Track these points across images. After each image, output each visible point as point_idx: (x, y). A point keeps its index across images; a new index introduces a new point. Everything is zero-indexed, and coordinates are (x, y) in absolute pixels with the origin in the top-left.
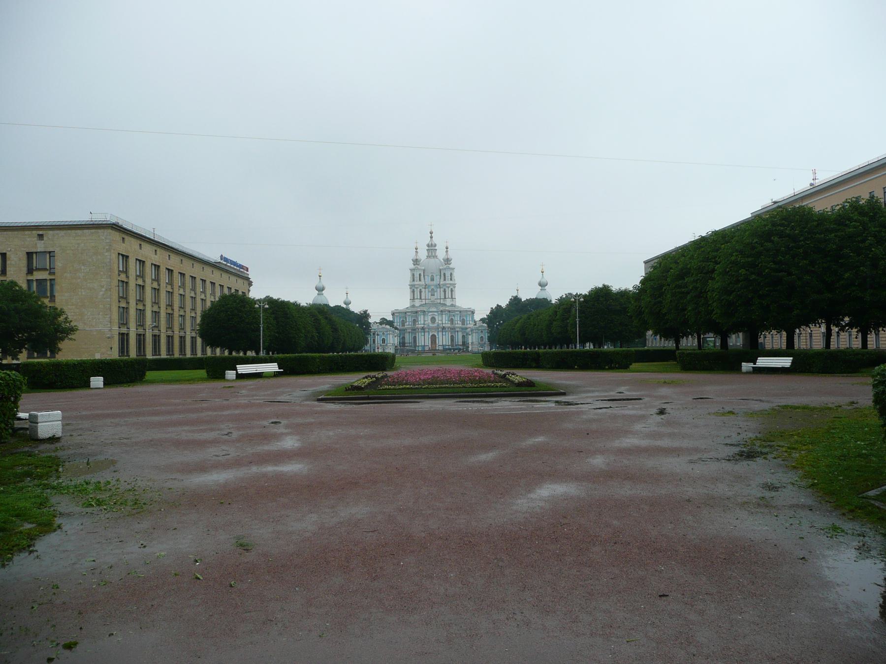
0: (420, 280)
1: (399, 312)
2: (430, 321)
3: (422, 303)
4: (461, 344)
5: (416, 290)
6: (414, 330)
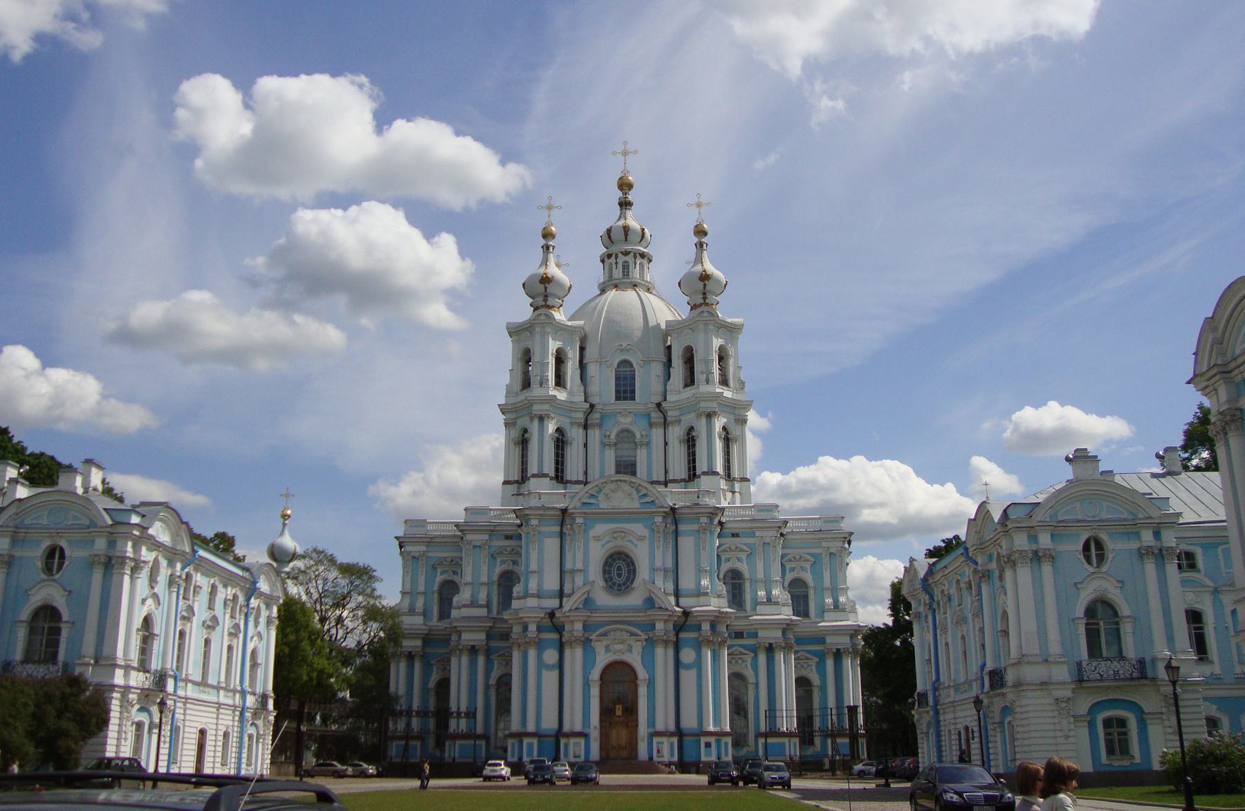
0: (560, 381)
2: (595, 572)
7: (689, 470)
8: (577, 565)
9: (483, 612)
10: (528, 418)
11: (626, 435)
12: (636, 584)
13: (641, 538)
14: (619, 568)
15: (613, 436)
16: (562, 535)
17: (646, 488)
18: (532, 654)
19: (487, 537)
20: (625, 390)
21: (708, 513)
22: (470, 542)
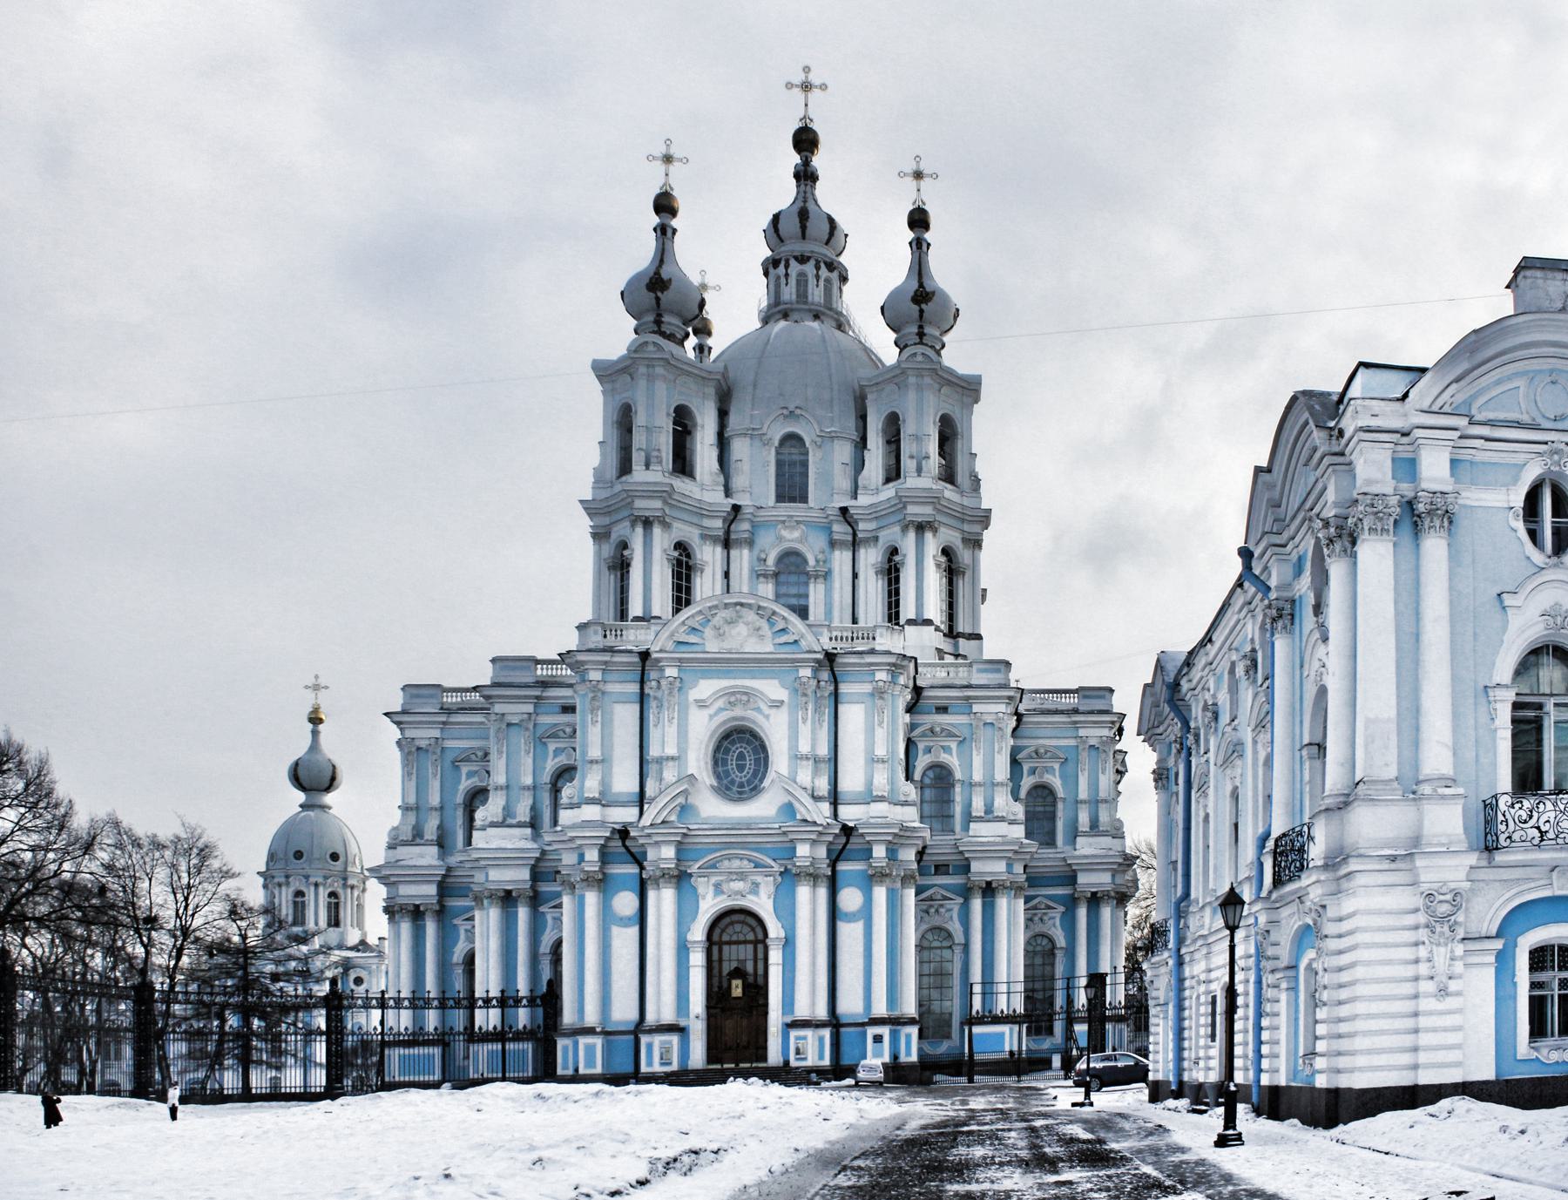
4: (1020, 1009)
8: (666, 751)
12: (766, 783)
13: (778, 704)
14: (741, 757)
17: (784, 618)
19: (530, 708)
21: (889, 664)
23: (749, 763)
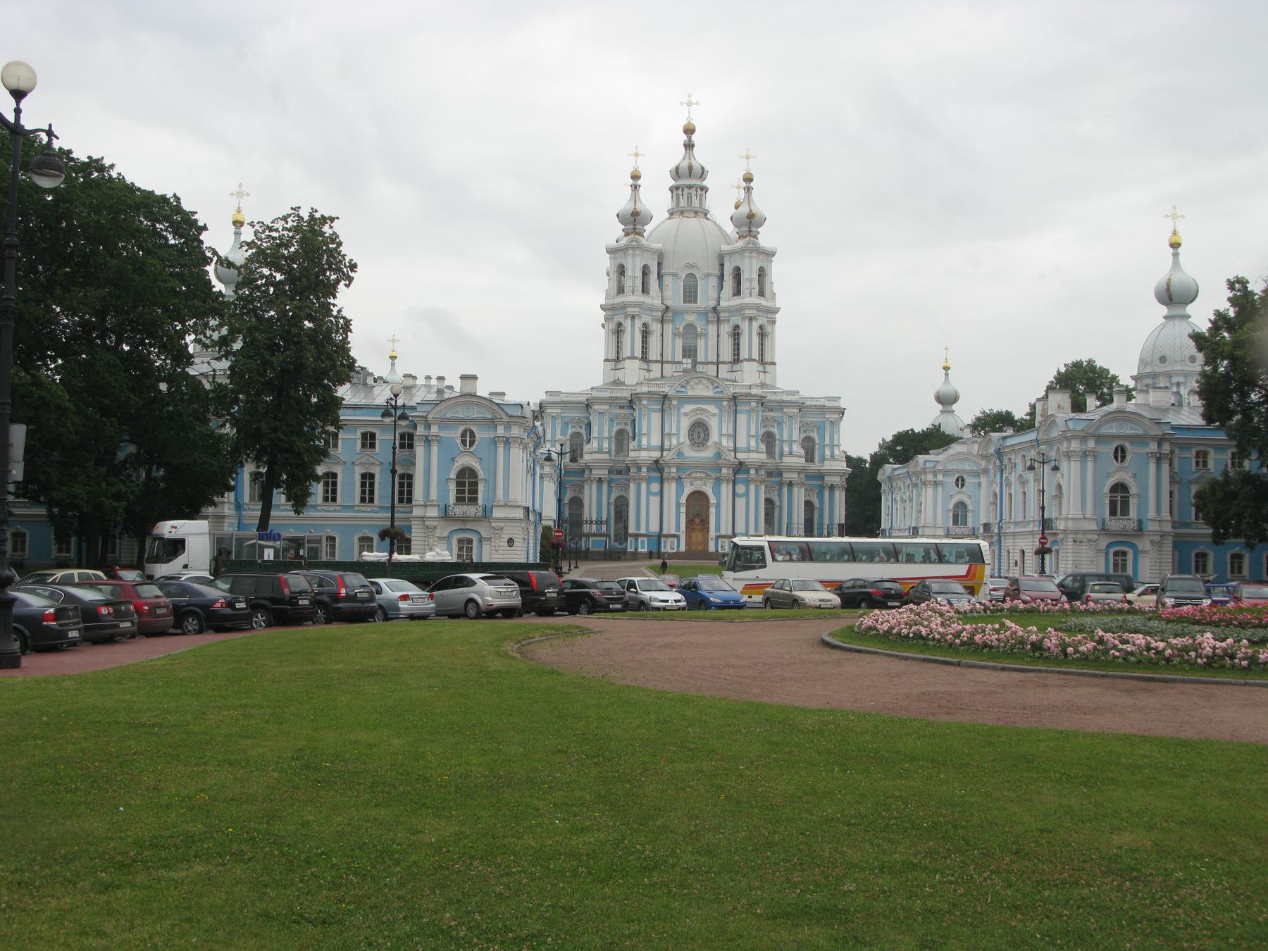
0: (645, 290)
1: (562, 402)
2: (684, 437)
3: (652, 375)
5: (627, 324)
6: (621, 472)
7: (734, 355)
9: (606, 456)
10: (623, 316)
11: (690, 327)
12: (709, 443)
14: (699, 433)
15: (681, 330)
16: (663, 411)
18: (644, 486)
20: (690, 294)
22: (596, 411)
23: (702, 435)
